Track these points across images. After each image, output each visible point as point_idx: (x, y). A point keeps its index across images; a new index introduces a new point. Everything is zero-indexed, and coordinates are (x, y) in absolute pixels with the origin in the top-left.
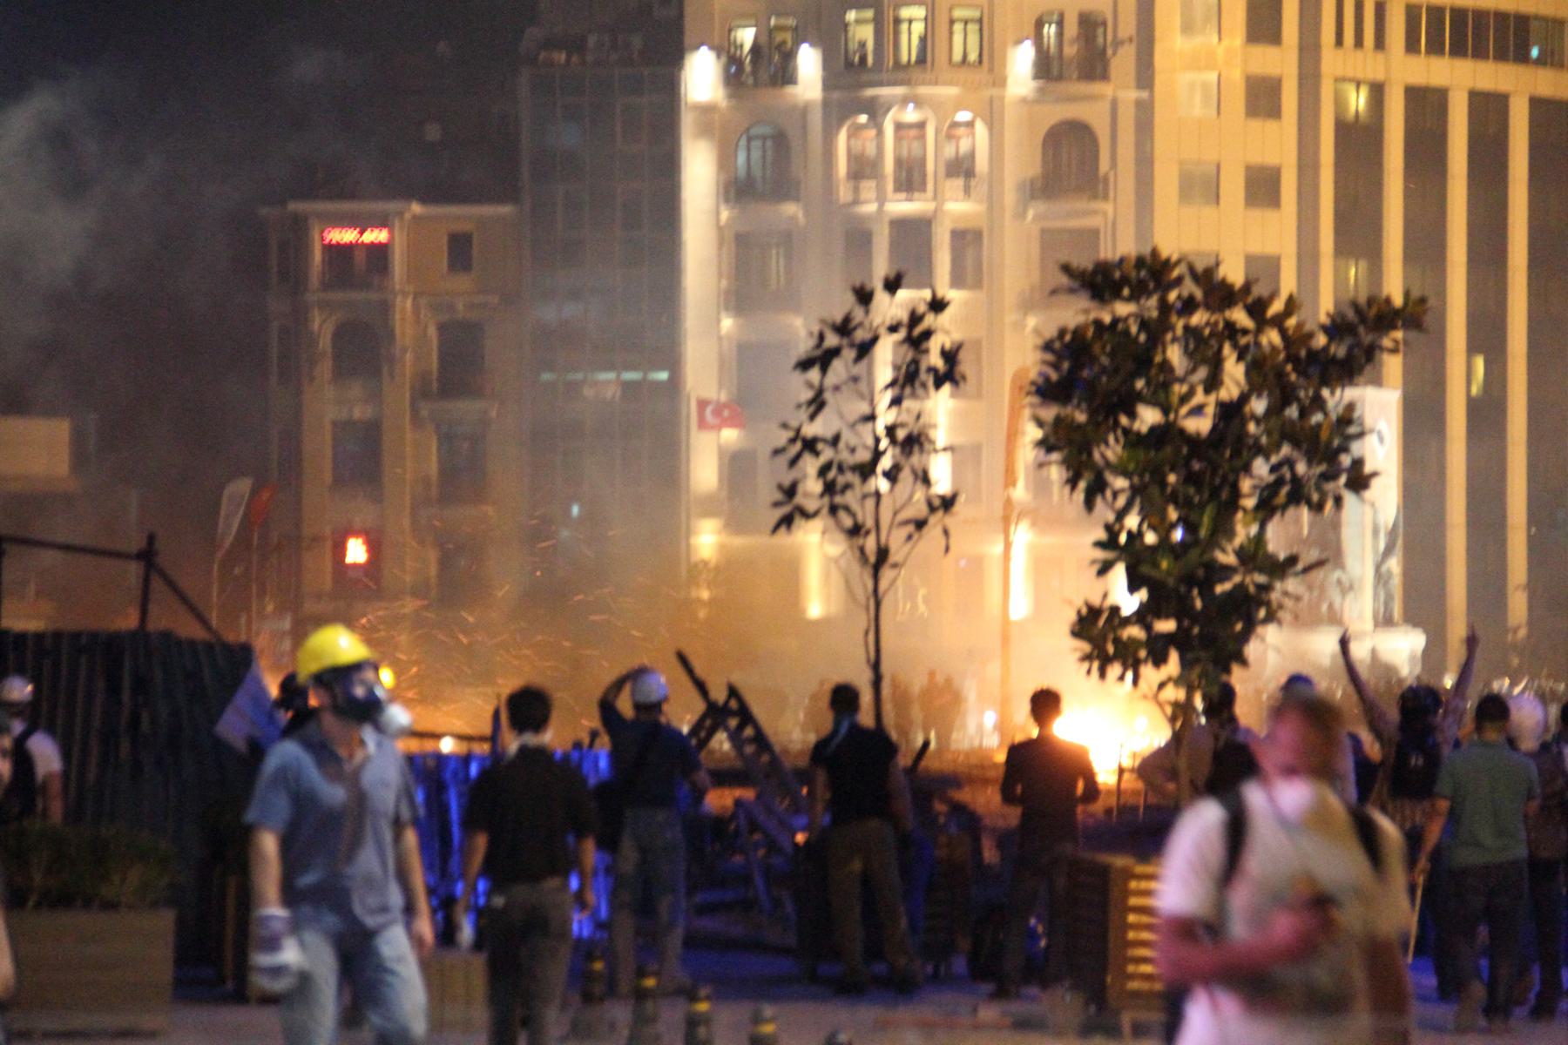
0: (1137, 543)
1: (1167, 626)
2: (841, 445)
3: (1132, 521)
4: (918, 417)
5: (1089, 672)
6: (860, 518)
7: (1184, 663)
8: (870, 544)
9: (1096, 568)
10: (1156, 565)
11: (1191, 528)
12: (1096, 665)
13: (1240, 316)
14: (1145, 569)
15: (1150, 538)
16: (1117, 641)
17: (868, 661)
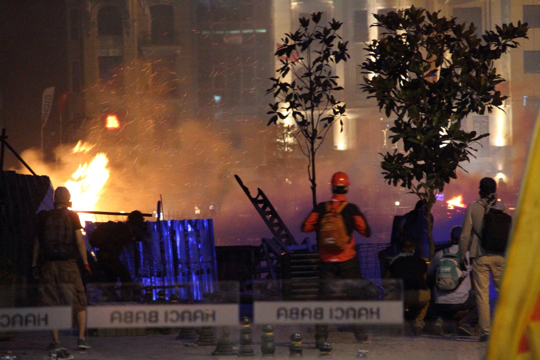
0: (408, 129)
1: (422, 162)
2: (296, 88)
3: (406, 119)
4: (330, 73)
5: (389, 183)
6: (305, 119)
7: (428, 179)
8: (310, 129)
9: (392, 139)
10: (415, 137)
11: (430, 122)
12: (392, 180)
13: (451, 33)
14: (410, 139)
15: (413, 126)
16: (401, 169)
17: (310, 179)
